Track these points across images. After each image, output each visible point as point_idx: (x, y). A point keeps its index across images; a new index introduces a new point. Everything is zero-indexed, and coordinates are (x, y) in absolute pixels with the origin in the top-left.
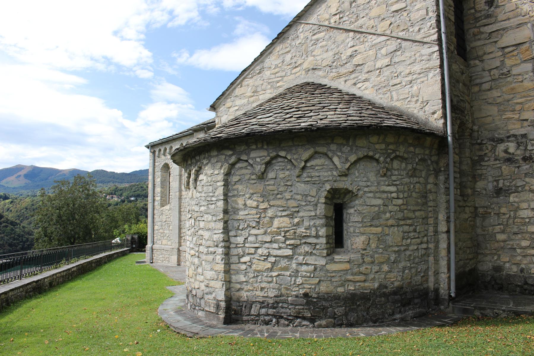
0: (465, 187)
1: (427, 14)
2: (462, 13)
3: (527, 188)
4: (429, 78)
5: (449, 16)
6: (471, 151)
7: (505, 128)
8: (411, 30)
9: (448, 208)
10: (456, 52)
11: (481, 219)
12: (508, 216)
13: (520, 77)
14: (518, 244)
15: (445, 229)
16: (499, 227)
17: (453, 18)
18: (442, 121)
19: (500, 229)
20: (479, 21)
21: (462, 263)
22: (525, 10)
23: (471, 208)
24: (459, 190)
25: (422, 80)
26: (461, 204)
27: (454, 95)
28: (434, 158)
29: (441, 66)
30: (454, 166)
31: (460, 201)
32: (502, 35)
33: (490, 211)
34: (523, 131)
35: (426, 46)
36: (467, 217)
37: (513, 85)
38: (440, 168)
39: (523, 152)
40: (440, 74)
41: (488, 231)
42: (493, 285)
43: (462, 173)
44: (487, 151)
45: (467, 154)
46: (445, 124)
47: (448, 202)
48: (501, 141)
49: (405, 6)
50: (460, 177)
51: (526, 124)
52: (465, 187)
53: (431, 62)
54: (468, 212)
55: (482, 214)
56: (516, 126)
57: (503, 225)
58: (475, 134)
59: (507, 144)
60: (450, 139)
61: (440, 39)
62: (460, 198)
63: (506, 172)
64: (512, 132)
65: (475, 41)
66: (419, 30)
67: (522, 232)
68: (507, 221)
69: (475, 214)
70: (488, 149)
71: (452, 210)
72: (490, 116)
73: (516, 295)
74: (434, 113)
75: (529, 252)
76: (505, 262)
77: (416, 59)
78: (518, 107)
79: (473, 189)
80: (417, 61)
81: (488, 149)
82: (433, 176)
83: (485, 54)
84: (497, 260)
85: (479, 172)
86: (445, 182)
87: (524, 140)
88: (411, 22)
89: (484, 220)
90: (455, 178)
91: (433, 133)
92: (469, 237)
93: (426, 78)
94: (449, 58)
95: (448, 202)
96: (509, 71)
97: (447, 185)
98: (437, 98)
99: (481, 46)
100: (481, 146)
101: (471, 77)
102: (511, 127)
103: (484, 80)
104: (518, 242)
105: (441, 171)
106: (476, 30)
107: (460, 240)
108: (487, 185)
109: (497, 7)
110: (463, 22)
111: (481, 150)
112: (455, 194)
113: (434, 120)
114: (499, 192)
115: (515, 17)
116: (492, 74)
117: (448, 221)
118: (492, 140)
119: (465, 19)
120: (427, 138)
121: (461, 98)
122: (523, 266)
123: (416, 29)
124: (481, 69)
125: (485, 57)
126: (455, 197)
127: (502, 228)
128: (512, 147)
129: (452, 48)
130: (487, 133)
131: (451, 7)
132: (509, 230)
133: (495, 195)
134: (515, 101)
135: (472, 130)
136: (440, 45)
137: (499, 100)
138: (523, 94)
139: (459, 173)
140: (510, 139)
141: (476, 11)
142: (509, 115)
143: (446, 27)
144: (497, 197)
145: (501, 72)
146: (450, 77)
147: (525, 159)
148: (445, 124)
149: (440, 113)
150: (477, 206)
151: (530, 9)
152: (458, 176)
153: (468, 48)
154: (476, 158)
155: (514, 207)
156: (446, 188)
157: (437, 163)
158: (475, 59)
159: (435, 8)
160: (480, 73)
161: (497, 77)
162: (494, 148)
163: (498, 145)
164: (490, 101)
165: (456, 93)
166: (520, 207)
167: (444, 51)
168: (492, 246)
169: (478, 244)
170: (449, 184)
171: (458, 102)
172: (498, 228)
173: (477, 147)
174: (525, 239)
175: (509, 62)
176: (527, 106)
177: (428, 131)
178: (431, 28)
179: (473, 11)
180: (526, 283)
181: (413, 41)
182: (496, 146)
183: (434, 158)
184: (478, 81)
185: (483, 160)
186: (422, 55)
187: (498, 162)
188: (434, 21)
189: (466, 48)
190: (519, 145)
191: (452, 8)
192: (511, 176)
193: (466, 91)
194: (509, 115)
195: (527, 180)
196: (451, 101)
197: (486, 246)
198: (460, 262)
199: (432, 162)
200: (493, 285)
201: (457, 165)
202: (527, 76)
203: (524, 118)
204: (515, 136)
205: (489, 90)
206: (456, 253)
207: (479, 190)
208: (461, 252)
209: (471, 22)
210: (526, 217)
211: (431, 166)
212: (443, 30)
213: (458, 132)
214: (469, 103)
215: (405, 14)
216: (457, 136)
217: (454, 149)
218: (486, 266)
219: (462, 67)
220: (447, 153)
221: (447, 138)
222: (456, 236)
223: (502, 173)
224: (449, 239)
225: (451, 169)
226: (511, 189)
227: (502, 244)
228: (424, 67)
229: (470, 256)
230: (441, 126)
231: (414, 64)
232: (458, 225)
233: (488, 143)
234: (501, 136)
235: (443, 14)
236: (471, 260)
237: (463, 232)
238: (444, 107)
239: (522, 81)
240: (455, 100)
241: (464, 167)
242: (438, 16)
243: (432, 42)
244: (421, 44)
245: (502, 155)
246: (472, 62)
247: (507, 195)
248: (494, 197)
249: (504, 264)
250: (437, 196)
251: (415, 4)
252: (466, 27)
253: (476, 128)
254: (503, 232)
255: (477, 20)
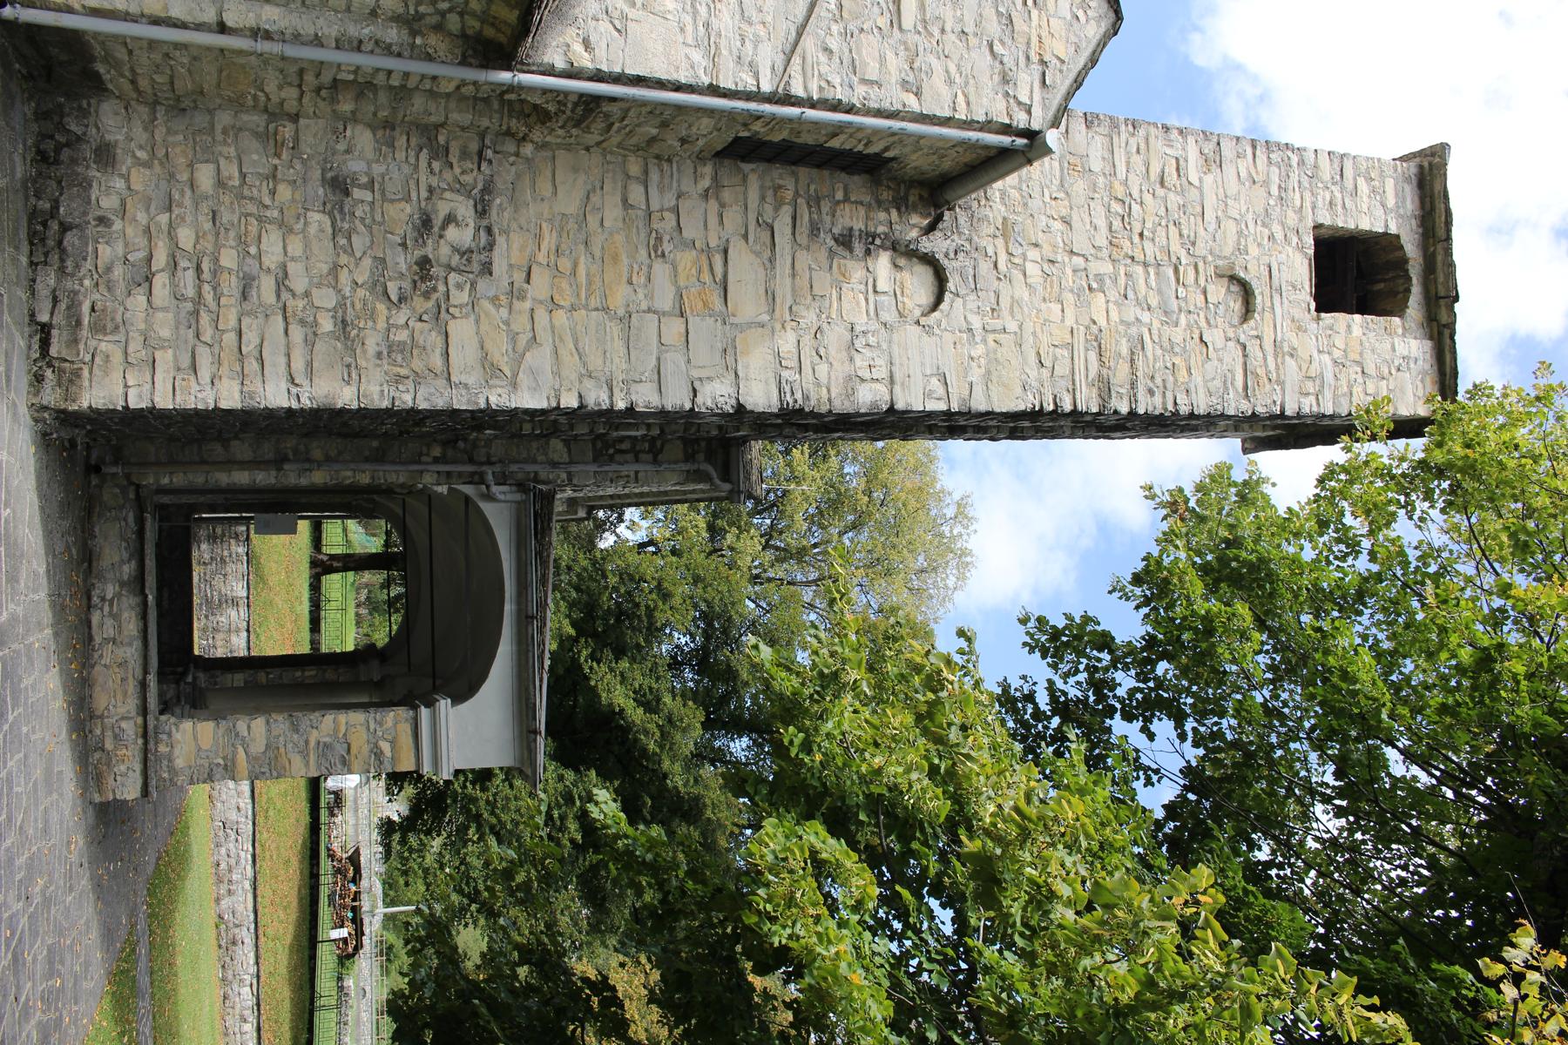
0: (360, 96)
1: (864, 81)
2: (843, 169)
3: (344, 259)
4: (688, 50)
5: (842, 137)
6: (463, 129)
7: (514, 226)
8: (835, 28)
9: (297, 38)
10: (746, 134)
11: (261, 129)
12: (267, 201)
13: (643, 280)
14: (183, 219)
15: (230, 20)
16: (237, 174)
17: (835, 143)
18: (560, 64)
19: (230, 178)
20: (810, 207)
21: (118, 55)
22: (804, 313)
23: (295, 103)
24: (351, 77)
25: (689, 28)
26: (309, 78)
27: (628, 110)
28: (453, 22)
29: (713, 90)
30: (423, 77)
31: (318, 75)
32: (757, 254)
33: (284, 156)
34: (499, 267)
35: (780, 60)
36: (267, 89)
37: (625, 261)
38: (423, 36)
39: (444, 260)
40: (692, 81)
41: (225, 143)
42: (52, 137)
43: (402, 93)
44: (457, 170)
45: (455, 116)
46: (550, 71)
47: (317, 41)
48: (482, 211)
49: (904, 26)
50: (391, 88)
51: (519, 277)
52: (360, 96)
53: (731, 65)
54: (283, 95)
55: (276, 133)
56: (515, 253)
57: (241, 186)
58: (510, 147)
59: (472, 225)
60: (505, 76)
61: (788, 100)
62: (326, 78)
63: (392, 213)
64: (501, 240)
65: (762, 187)
66: (828, 50)
67: (218, 234)
68: (251, 199)
69: (276, 114)
70: (462, 173)
71: (292, 51)
72: (555, 193)
73: (27, 198)
74: (587, 44)
75: (160, 244)
76: (128, 180)
77: (750, 24)
78: (565, 264)
79: (354, 118)
80: (744, 26)
81: (462, 173)
82: (401, 11)
83: (722, 205)
84: (134, 156)
85: (401, 141)
86: (377, 42)
87: (476, 267)
88: (856, 32)
89: (256, 135)
90: (390, 72)
91: (527, 32)
92: (206, 86)
93: (690, 41)
94: (731, 115)
95: (317, 41)
96: (663, 255)
97: (368, 46)
98: (628, 62)
99: (746, 199)
100: (476, 158)
101: (669, 160)
102: (517, 239)
103: (654, 192)
104: (189, 219)
105: (414, 33)
106: (789, 195)
107: (195, 58)
108: (360, 158)
109: (832, 254)
110: (819, 166)
111: (464, 154)
112: (339, 65)
113: (568, 40)
114: (340, 186)
115: (794, 290)
116: (666, 214)
117: (256, 33)
118: (488, 189)
119: (826, 173)
120: (517, 12)
121: (617, 125)
122: (118, 225)
123: (834, 44)
124: (684, 188)
125: (713, 205)
126: (330, 64)
127: (231, 183)
128: (462, 236)
129: (757, 127)
130: (510, 178)
131: (866, 145)
132: (227, 199)
133: (329, 175)
134: (582, 259)
135: (524, 139)
136: (771, 99)
137: (593, 221)
138: (597, 279)
139: (403, 87)
140: (482, 233)
141: (838, 202)
142: (549, 241)
143: (816, 124)
144: (323, 179)
145: (666, 238)
146: (680, 108)
147: (424, 263)
148: (550, 71)
149: (585, 61)
150: (302, 121)
151: (803, 325)
152: (395, 82)
153: (747, 167)
154: (442, 140)
155: (292, 221)
156: (361, 42)
157: (438, 28)
158: (715, 179)
159: (874, 105)
160: (675, 184)
161: (655, 226)
162: (463, 189)
163: (472, 202)
164: (595, 199)
165: (631, 113)
166: (292, 237)
167: (752, 106)
168: (178, 150)
169: (184, 110)
170: (372, 52)
171: (607, 116)
172: (231, 170)
173: (474, 146)
174: (198, 238)
175: (686, 259)
176: (564, 285)
177: (537, 18)
178: (824, 84)
179: (839, 195)
180: (65, 228)
181: (804, 26)
182: (469, 196)
183: (453, 22)
184: (654, 176)
185: (434, 156)
186: (757, 42)
187: (424, 194)
188: (840, 94)
189: (749, 162)
190: (466, 253)
191: (860, 148)
192: (380, 224)
193: (634, 141)
194: (549, 241)
195: (367, 262)
196: (613, 99)
197: (176, 133)
198: (124, 50)
199: (443, 14)
200: (52, 137)
201: (427, 85)
202: (641, 296)
203: (533, 275)
204: (490, 246)
205: (625, 201)
206: (152, 44)
207: (348, 133)
208: (157, 57)
209: (812, 187)
210: (263, 247)
211: (430, 10)
212: (811, 114)
213: (522, 101)
214: (598, 144)
215: (883, 22)
216: (513, 97)
217: (475, 83)
218: (111, 122)
219: (701, 143)
220: (464, 63)
221: (509, 68)
222: (209, 49)
223: (392, 201)
224: (199, 27)
225: (418, 67)
226: (343, 220)
227: (185, 177)
228: (723, 43)
229: (143, 83)
230: (547, 59)
231: (738, 17)
232: (242, 60)
233: (481, 177)
234: (494, 212)
235: (850, 123)
236: (133, 82)
237: (221, 71)
238: (599, 76)
239: (630, 283)
240: (614, 109)
241: (419, 102)
242: (850, 110)
243: (786, 78)
244: (788, 48)
245: (443, 209)
246: (708, 170)
247: (329, 206)
248: (324, 171)
249: (121, 176)
250: (336, 11)
251: (902, 53)
252: (803, 172)
253: (528, 150)
254: (220, 183)
255: (815, 201)
